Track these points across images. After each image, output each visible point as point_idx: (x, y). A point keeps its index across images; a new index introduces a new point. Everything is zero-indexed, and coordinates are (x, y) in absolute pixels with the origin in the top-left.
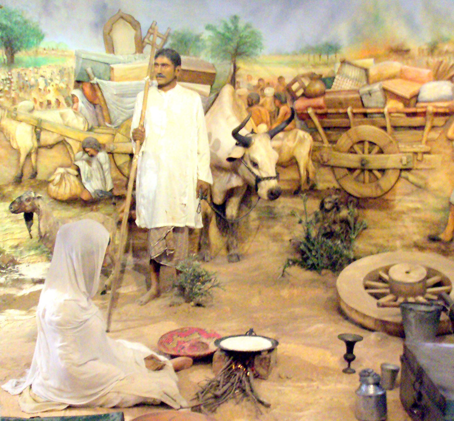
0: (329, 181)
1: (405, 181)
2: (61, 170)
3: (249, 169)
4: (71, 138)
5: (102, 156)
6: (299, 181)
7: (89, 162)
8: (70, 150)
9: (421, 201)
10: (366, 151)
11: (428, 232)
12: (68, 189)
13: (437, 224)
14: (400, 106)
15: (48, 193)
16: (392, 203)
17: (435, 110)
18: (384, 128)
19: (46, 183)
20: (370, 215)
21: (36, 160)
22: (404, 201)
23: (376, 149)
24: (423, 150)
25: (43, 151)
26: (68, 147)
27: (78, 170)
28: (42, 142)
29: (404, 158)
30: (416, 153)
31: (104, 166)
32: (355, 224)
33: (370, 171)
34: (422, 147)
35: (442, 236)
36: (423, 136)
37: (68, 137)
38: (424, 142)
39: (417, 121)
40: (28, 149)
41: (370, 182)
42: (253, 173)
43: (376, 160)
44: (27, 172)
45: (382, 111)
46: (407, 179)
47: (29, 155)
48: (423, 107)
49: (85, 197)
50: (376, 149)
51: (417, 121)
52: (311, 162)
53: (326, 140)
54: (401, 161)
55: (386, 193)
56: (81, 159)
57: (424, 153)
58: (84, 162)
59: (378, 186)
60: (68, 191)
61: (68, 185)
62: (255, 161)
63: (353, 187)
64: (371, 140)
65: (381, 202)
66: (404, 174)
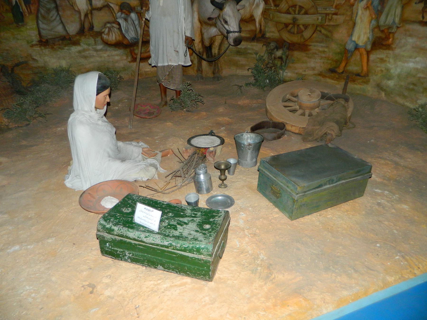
0: (273, 32)
1: (319, 32)
2: (109, 25)
3: (222, 24)
4: (112, 3)
5: (133, 15)
6: (256, 31)
7: (126, 20)
8: (113, 11)
9: (327, 47)
10: (297, 12)
11: (329, 67)
12: (113, 37)
13: (336, 61)
15: (102, 39)
16: (309, 47)
19: (100, 34)
20: (297, 54)
21: (92, 18)
22: (316, 47)
23: (303, 11)
24: (333, 12)
25: (95, 12)
26: (111, 9)
27: (119, 24)
28: (94, 6)
29: (320, 18)
30: (327, 14)
31: (135, 22)
32: (286, 60)
33: (298, 26)
34: (333, 10)
37: (110, 3)
40: (85, 11)
42: (225, 28)
44: (87, 25)
46: (320, 31)
47: (86, 15)
49: (125, 42)
50: (303, 11)
52: (263, 19)
53: (272, 5)
54: (318, 19)
55: (307, 40)
56: (121, 18)
58: (123, 19)
59: (302, 36)
60: (114, 38)
61: (114, 34)
62: (226, 20)
63: (286, 36)
64: (301, 5)
65: (303, 47)
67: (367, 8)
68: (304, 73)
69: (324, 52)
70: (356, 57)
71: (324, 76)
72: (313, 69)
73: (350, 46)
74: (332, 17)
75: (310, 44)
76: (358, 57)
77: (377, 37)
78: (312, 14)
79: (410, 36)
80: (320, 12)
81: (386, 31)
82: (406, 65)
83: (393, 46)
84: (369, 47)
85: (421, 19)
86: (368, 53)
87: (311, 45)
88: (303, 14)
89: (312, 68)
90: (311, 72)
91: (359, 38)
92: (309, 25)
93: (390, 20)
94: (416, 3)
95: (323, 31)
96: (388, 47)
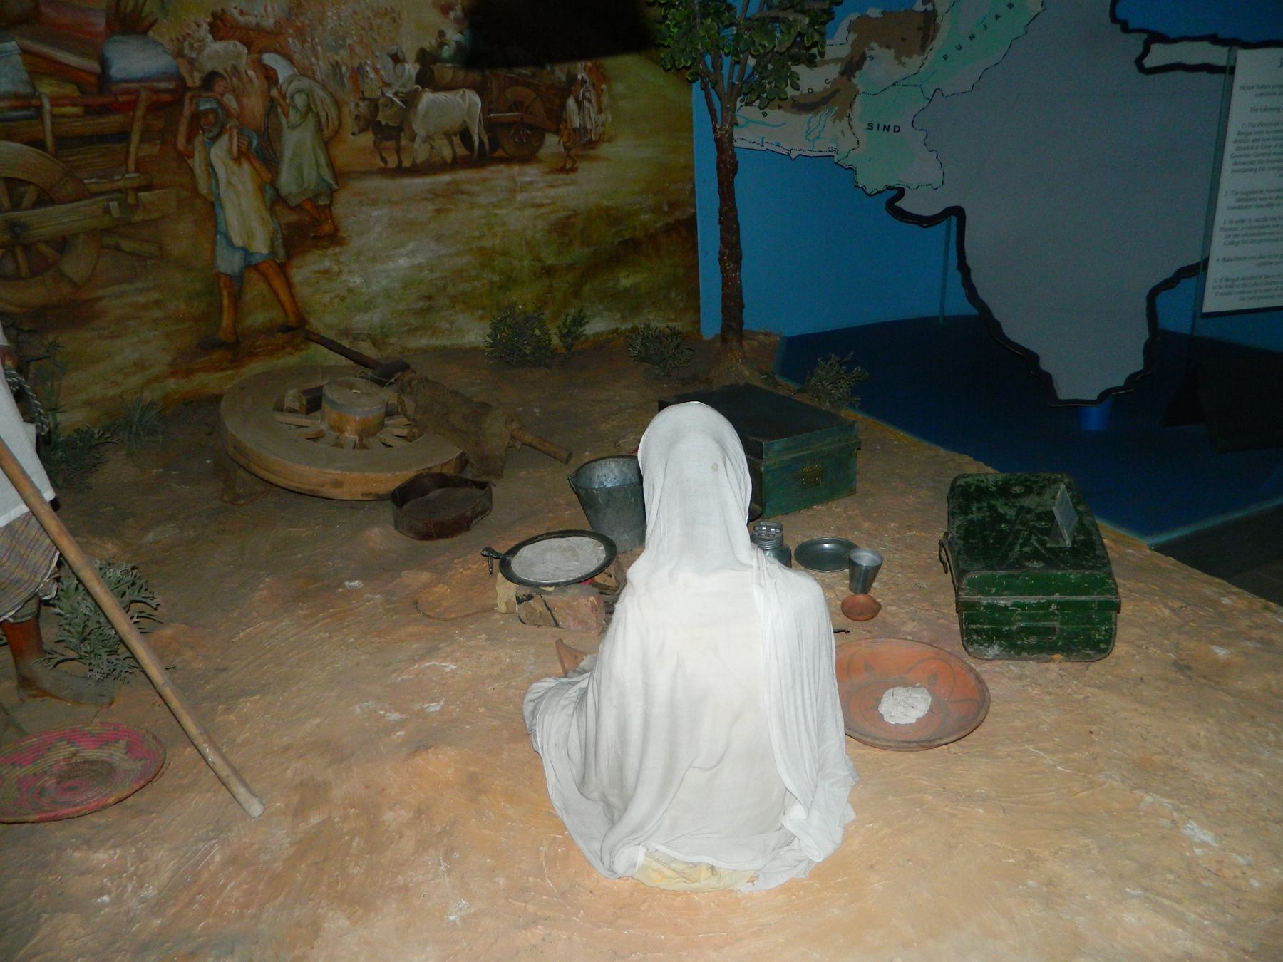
14: (70, 90)
17: (155, 98)
18: (38, 144)
23: (30, 195)
34: (132, 177)
35: (221, 336)
36: (128, 152)
38: (132, 166)
39: (112, 122)
41: (34, 274)
43: (48, 221)
45: (34, 102)
46: (118, 248)
48: (126, 92)
51: (112, 122)
54: (107, 210)
57: (138, 189)
59: (63, 276)
66: (108, 240)
67: (239, 157)
68: (112, 392)
69: (157, 303)
70: (256, 289)
71: (189, 373)
72: (140, 366)
73: (229, 263)
74: (137, 198)
75: (100, 293)
76: (262, 286)
77: (289, 225)
78: (71, 201)
79: (375, 203)
80: (94, 188)
81: (308, 207)
82: (391, 265)
83: (342, 234)
84: (281, 253)
85: (382, 165)
86: (283, 269)
87: (100, 299)
88: (26, 209)
89: (135, 364)
90: (137, 380)
91: (250, 235)
92: (75, 235)
93: (310, 178)
94: (353, 134)
95: (127, 245)
96: (335, 238)
